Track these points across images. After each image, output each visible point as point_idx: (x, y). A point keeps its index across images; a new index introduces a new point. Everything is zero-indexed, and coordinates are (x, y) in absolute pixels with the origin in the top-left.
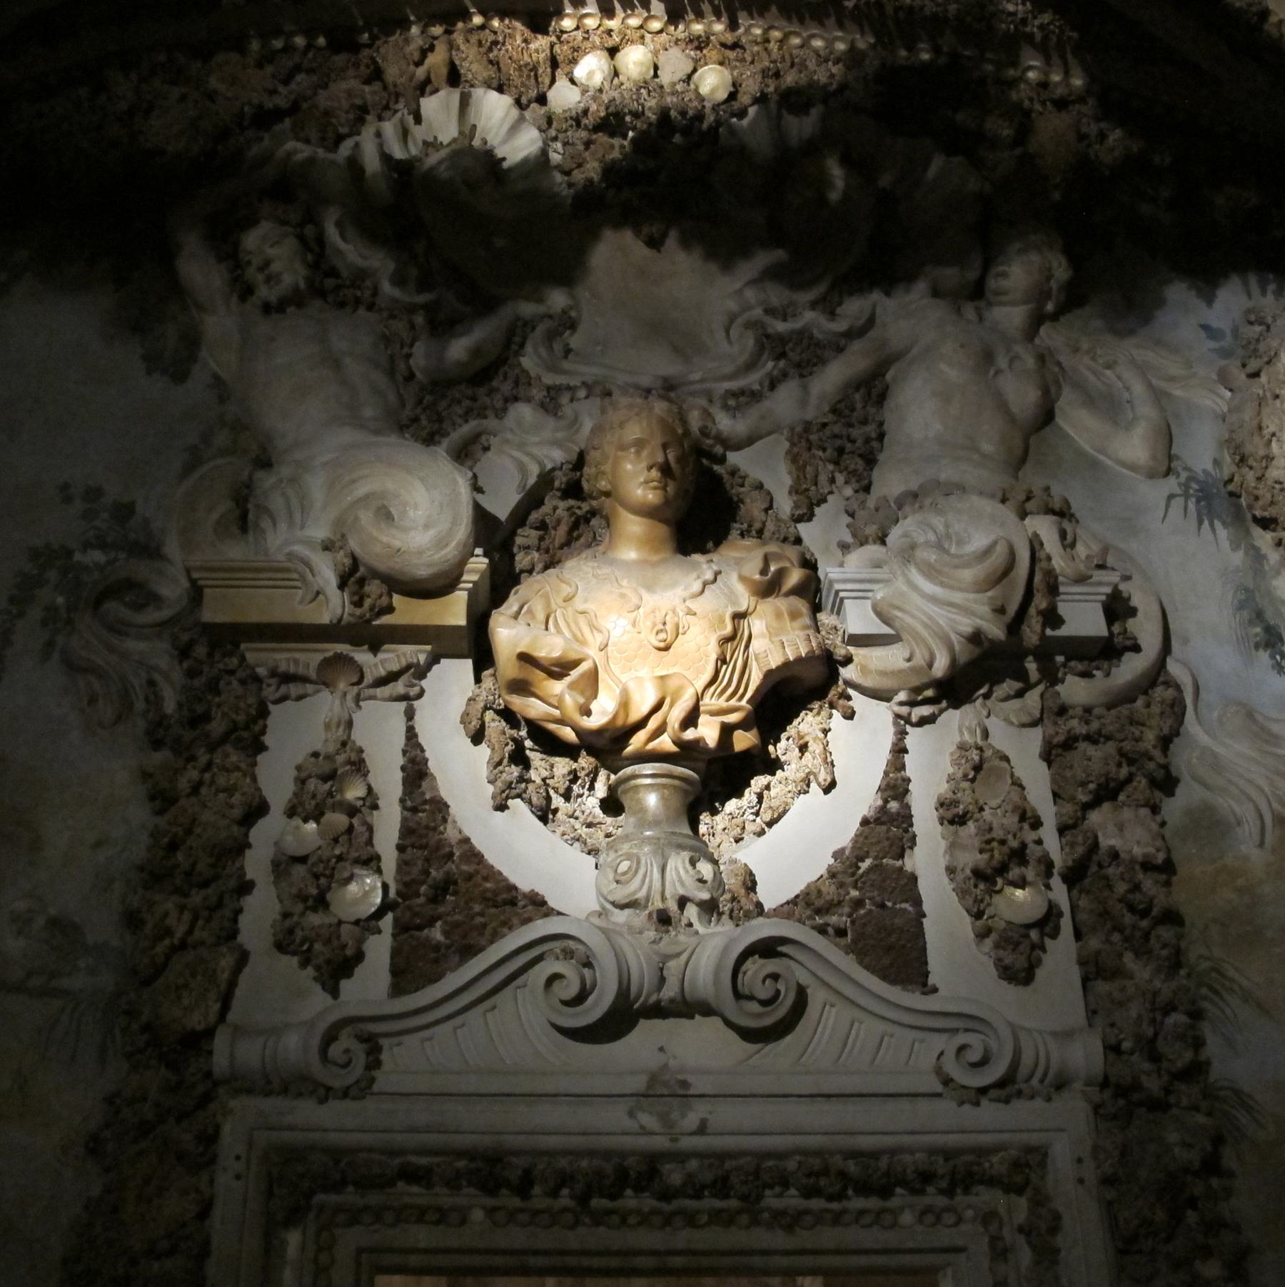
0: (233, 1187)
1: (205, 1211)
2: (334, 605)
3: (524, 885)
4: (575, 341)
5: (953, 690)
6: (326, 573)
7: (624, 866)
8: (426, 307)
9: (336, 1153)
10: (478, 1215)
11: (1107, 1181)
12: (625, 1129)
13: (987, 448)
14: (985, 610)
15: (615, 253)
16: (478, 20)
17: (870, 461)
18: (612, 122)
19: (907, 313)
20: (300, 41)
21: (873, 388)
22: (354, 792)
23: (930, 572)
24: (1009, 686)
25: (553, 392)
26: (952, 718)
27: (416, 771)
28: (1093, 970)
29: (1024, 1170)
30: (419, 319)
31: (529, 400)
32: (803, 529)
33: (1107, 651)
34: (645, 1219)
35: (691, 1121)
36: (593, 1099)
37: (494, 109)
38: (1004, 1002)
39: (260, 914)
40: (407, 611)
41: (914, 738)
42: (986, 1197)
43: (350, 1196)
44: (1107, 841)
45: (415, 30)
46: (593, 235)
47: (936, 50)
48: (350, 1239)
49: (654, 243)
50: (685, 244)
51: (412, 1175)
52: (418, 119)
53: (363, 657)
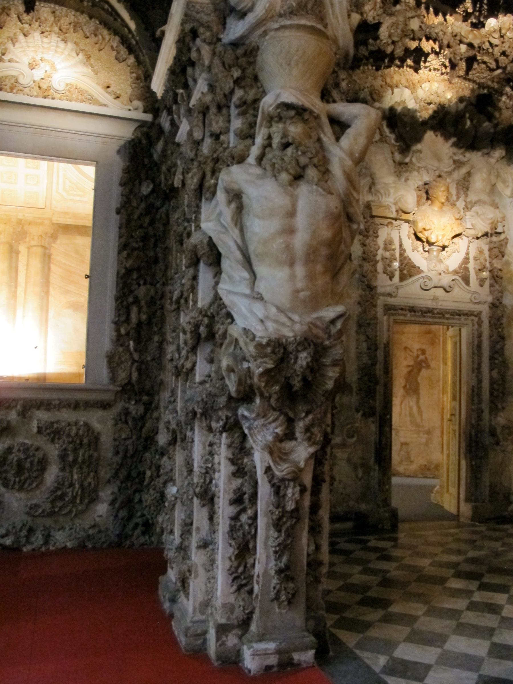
0: (380, 310)
1: (377, 312)
2: (394, 215)
3: (417, 265)
4: (421, 155)
5: (478, 238)
6: (394, 209)
7: (434, 264)
8: (398, 146)
9: (392, 305)
10: (409, 315)
11: (490, 317)
12: (431, 305)
13: (487, 191)
14: (489, 228)
15: (429, 135)
16: (405, 68)
17: (468, 189)
18: (430, 104)
19: (475, 158)
20: (370, 68)
21: (469, 174)
22: (393, 247)
23: (482, 220)
24: (485, 237)
25: (419, 168)
26: (477, 241)
27: (401, 245)
28: (491, 286)
29: (478, 315)
30: (396, 148)
31: (415, 170)
32: (458, 203)
33: (500, 233)
34: (430, 317)
35: (440, 304)
36: (425, 300)
37: (407, 92)
38: (478, 289)
39: (380, 267)
40: (405, 216)
41: (471, 244)
42: (473, 317)
43: (392, 312)
44: (495, 265)
45: (392, 68)
46: (425, 132)
47: (488, 91)
48: (392, 318)
49: (436, 136)
50: (441, 135)
51: (402, 309)
52: (393, 93)
53: (393, 222)
